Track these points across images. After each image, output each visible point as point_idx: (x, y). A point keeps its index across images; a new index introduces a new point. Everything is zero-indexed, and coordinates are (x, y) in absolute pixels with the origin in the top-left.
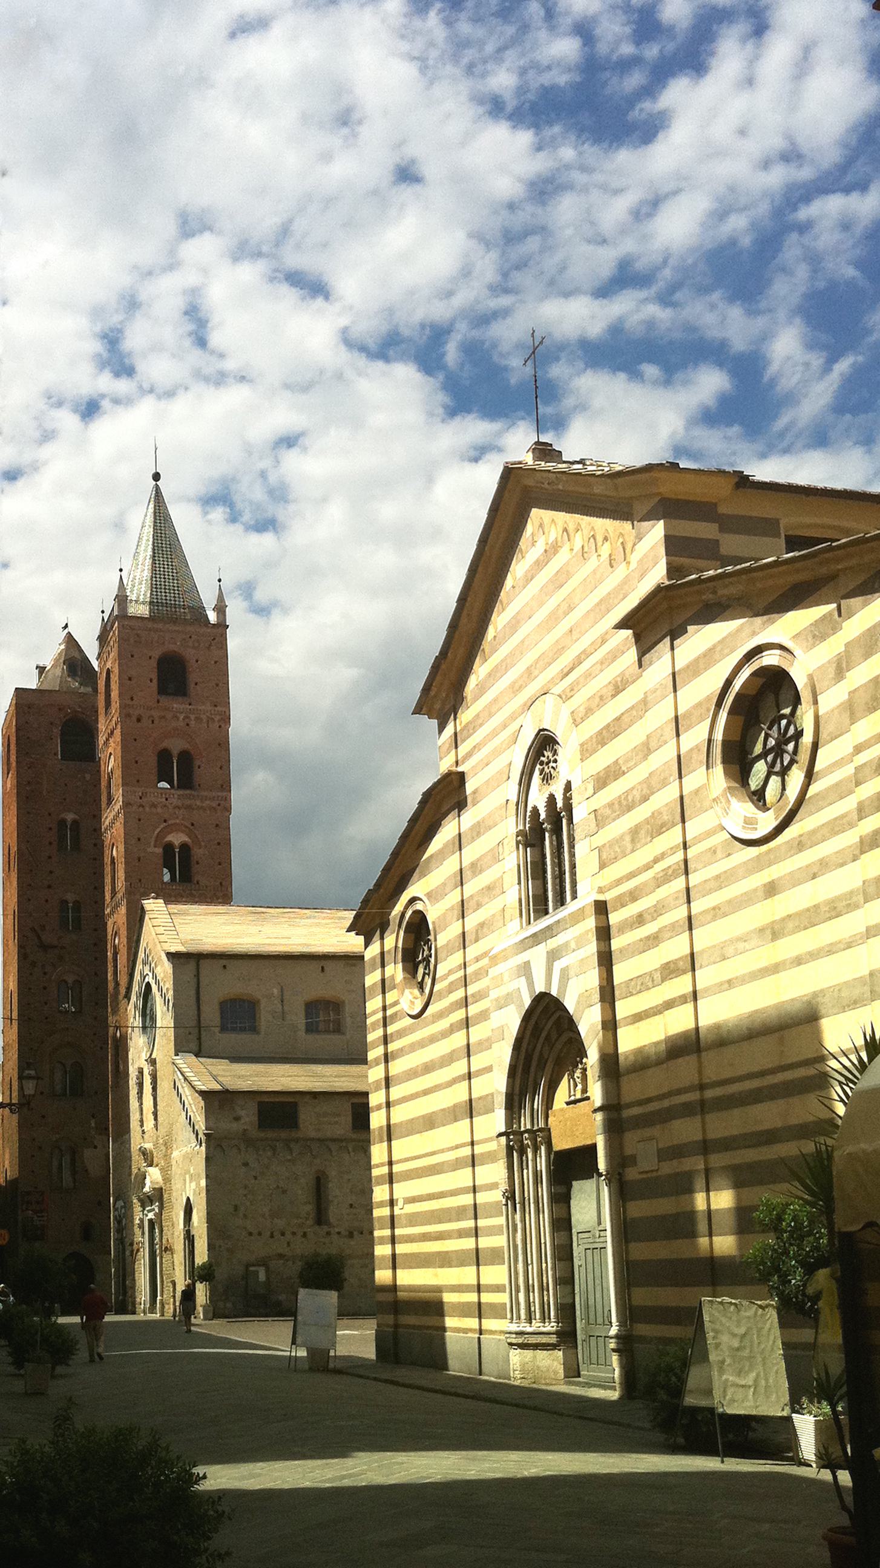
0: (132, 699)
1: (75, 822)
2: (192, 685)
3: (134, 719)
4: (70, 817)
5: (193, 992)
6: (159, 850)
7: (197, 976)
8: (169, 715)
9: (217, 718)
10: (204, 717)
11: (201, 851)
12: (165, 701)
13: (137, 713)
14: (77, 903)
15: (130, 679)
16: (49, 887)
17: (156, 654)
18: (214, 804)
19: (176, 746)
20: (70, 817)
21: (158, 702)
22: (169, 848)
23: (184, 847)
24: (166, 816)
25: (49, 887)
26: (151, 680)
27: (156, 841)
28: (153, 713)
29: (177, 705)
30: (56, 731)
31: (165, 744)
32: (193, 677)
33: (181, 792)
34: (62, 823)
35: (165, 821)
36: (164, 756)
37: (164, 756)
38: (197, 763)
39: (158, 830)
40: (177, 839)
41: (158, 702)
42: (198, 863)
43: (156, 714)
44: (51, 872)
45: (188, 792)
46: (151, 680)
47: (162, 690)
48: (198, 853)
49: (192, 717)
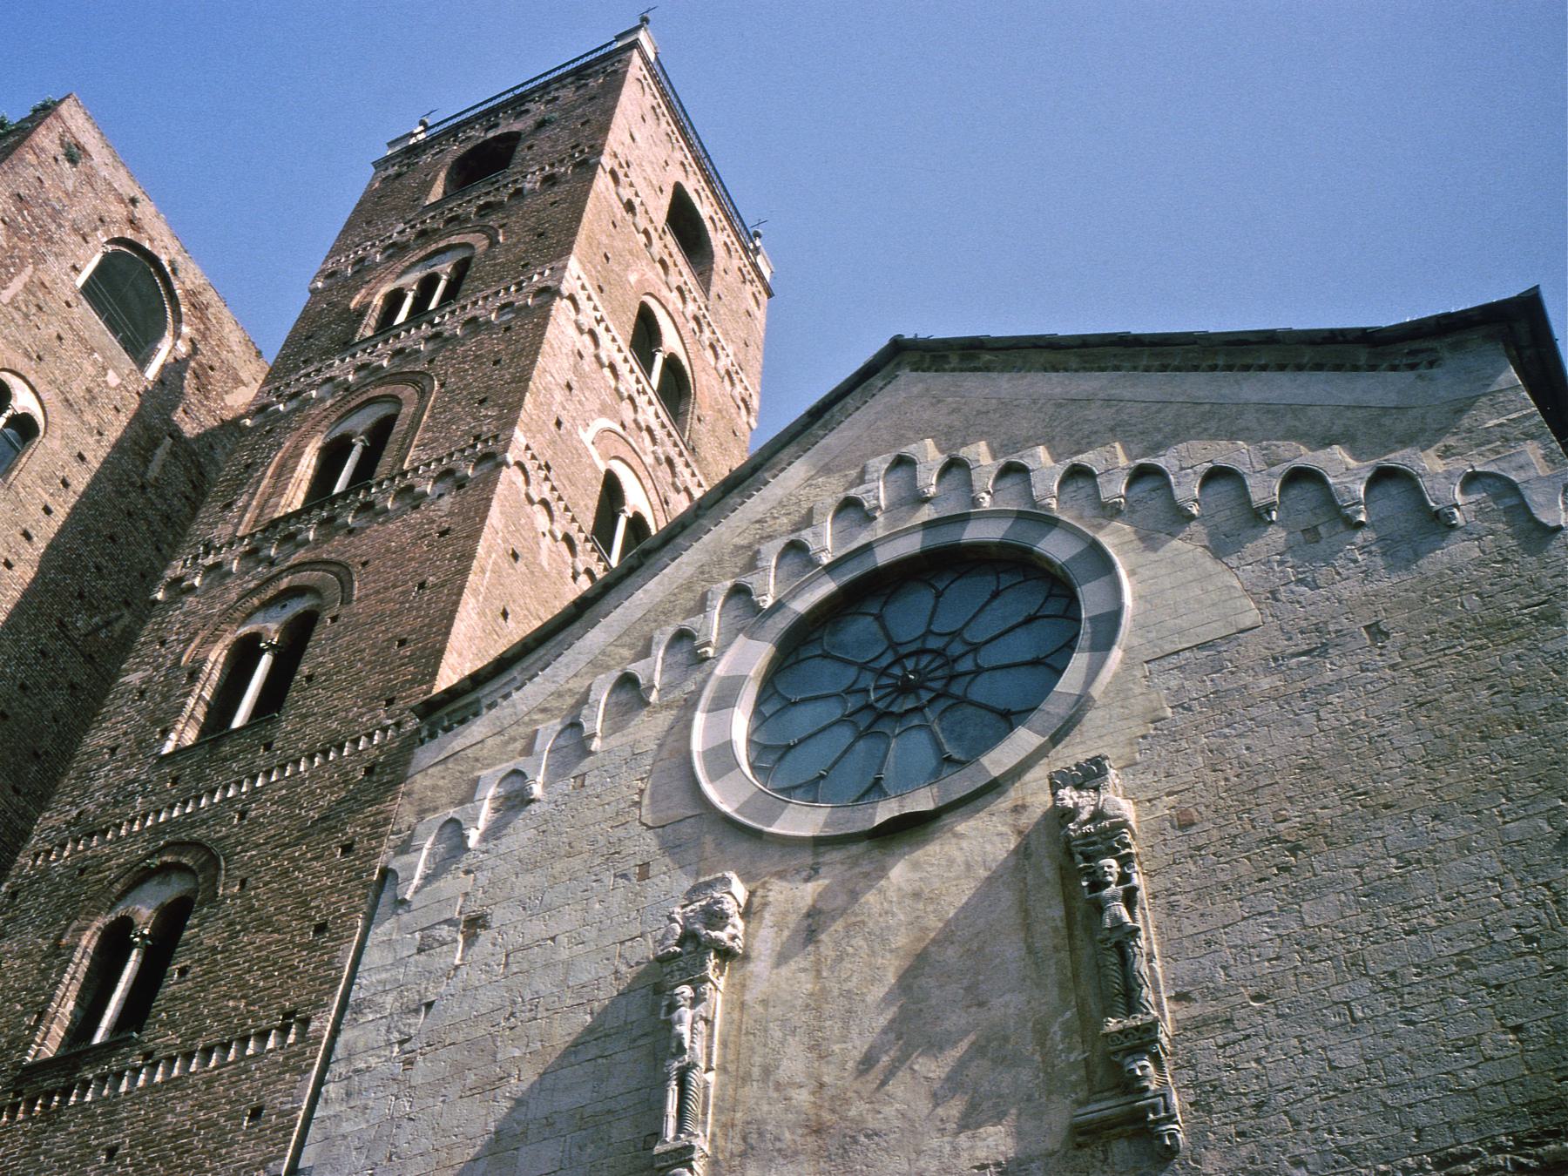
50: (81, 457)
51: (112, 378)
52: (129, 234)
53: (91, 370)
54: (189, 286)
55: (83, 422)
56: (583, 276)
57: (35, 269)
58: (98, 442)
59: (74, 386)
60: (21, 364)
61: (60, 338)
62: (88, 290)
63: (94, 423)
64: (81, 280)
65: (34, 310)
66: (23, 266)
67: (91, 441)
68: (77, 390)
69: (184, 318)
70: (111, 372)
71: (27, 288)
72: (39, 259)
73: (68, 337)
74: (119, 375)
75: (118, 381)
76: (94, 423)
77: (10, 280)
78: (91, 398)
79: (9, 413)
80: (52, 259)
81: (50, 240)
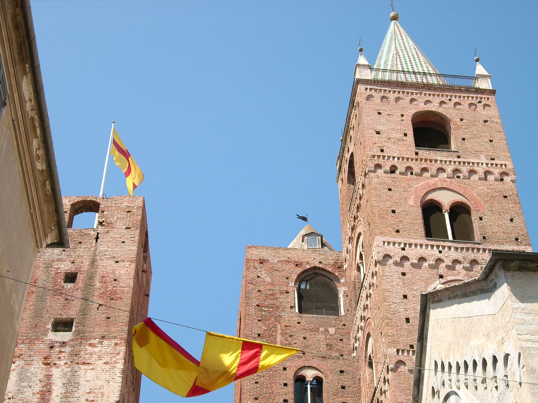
0: (382, 151)
3: (388, 168)
9: (497, 171)
12: (424, 153)
15: (378, 133)
19: (446, 199)
21: (417, 154)
26: (406, 135)
28: (410, 164)
31: (430, 197)
34: (300, 380)
35: (441, 277)
36: (430, 209)
37: (430, 209)
41: (417, 154)
46: (406, 135)
50: (342, 372)
51: (332, 330)
52: (299, 270)
53: (322, 337)
54: (332, 262)
55: (334, 359)
56: (385, 239)
57: (280, 324)
58: (343, 359)
60: (300, 363)
61: (305, 338)
63: (337, 354)
65: (290, 339)
66: (275, 327)
67: (341, 362)
69: (339, 277)
70: (330, 329)
72: (278, 319)
76: (337, 354)
77: (276, 338)
78: (329, 346)
80: (282, 313)
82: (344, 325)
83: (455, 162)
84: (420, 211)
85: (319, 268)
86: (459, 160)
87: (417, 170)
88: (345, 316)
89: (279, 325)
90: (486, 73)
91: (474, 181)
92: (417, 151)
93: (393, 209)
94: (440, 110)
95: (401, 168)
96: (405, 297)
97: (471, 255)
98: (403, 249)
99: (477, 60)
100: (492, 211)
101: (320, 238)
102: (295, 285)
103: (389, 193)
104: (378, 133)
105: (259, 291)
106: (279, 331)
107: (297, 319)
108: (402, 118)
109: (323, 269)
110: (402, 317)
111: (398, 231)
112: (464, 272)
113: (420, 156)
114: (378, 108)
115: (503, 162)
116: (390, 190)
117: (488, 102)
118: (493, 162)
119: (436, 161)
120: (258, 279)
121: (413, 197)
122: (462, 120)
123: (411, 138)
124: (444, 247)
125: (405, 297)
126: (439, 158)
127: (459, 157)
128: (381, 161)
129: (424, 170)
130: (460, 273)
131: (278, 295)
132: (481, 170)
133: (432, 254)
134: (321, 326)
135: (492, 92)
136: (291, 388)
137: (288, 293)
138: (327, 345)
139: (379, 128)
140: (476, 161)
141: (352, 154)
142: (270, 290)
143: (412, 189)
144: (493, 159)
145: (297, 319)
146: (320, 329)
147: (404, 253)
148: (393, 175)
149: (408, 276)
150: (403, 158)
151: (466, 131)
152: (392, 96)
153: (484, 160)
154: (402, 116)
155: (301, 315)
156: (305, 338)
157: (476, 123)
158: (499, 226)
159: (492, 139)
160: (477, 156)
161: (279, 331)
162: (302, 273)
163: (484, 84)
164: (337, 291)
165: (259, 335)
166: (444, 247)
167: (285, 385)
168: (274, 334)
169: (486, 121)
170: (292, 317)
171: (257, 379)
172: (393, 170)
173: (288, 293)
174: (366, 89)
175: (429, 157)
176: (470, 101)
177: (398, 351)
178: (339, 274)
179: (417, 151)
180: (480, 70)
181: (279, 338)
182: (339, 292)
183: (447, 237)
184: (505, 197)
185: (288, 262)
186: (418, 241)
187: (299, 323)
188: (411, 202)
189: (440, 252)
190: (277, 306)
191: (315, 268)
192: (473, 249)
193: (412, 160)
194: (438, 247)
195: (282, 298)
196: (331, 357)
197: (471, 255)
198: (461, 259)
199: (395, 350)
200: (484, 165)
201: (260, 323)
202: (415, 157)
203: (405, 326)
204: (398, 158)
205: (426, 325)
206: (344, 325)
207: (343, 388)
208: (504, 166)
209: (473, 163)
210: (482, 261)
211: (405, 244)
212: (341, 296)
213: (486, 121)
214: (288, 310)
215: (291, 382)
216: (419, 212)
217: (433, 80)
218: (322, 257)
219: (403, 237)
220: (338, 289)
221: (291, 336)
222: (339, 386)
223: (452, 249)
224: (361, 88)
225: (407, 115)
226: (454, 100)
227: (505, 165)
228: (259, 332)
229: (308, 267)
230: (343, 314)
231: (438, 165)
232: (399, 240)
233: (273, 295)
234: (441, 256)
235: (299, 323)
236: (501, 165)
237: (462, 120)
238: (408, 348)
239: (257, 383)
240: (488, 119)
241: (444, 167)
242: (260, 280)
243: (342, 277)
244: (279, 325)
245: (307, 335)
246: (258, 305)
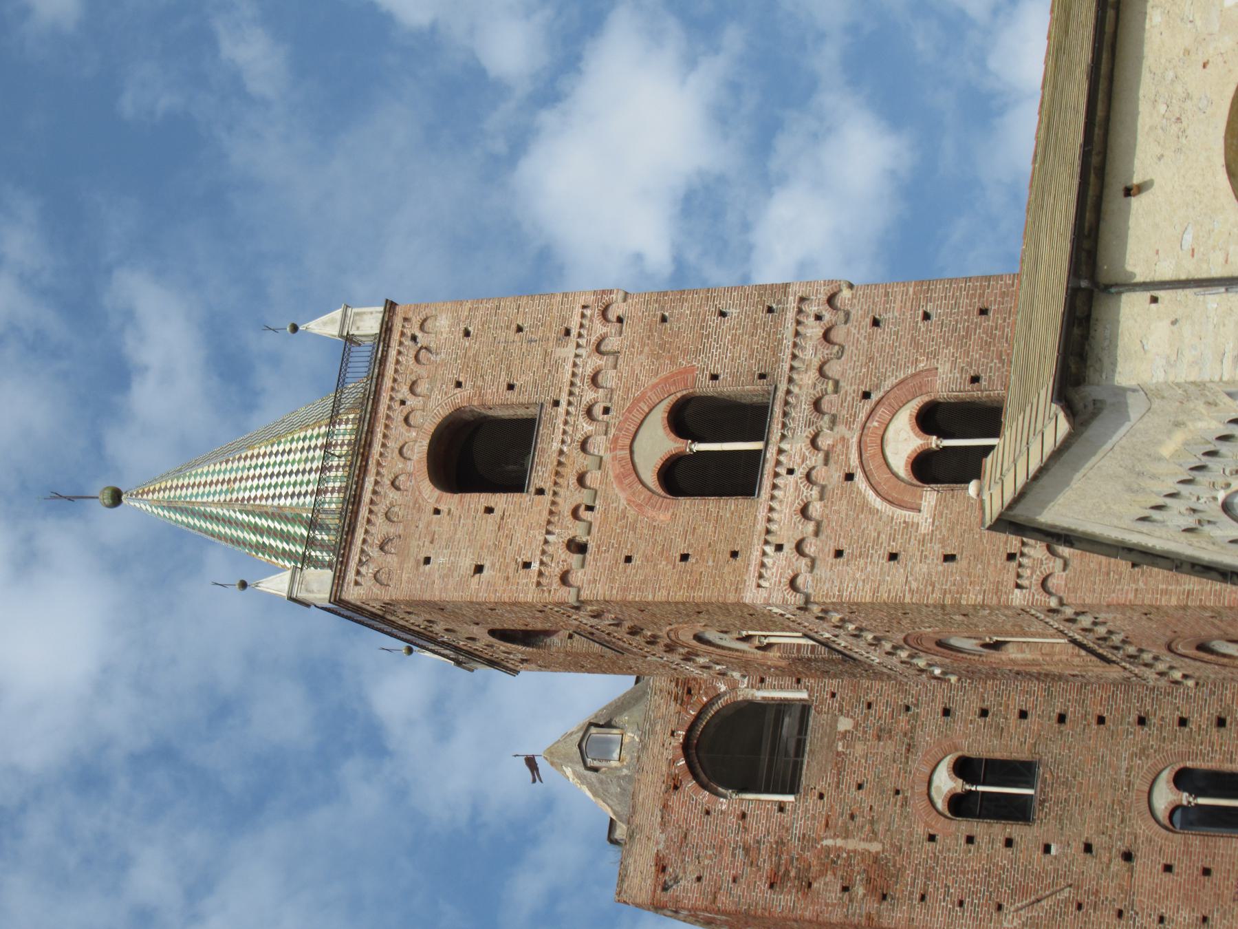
0: (527, 565)
1: (964, 768)
2: (512, 397)
3: (575, 558)
4: (945, 783)
5: (1214, 300)
6: (930, 497)
7: (1154, 286)
8: (578, 461)
9: (599, 328)
10: (592, 363)
11: (944, 368)
12: (540, 476)
13: (563, 554)
14: (1183, 779)
15: (479, 569)
16: (1128, 857)
17: (430, 493)
18: (814, 331)
19: (658, 443)
20: (945, 783)
21: (540, 492)
22: (926, 468)
23: (929, 419)
24: (836, 475)
25: (1128, 857)
26: (489, 510)
27: (900, 505)
28: (565, 508)
29: (550, 444)
30: (728, 803)
31: (650, 476)
32: (491, 396)
33: (776, 431)
34: (959, 805)
35: (849, 477)
36: (678, 478)
37: (678, 478)
38: (705, 387)
39: (877, 503)
40: (904, 441)
41: (540, 492)
42: (975, 379)
43: (571, 496)
44: (1088, 848)
45: (778, 410)
46: (489, 510)
47: (512, 480)
48: (947, 384)
49: (589, 395)
50: (946, 712)
51: (845, 724)
52: (690, 784)
53: (860, 748)
54: (674, 708)
55: (913, 727)
57: (822, 839)
59: (888, 752)
61: (860, 787)
62: (792, 787)
64: (790, 798)
65: (859, 820)
66: (828, 850)
67: (922, 711)
68: (888, 748)
69: (712, 694)
71: (847, 835)
73: (850, 780)
74: (836, 721)
75: (841, 718)
76: (903, 718)
77: (855, 851)
79: (968, 787)
81: (781, 843)
82: (833, 695)
83: (568, 413)
84: (685, 503)
85: (687, 738)
86: (563, 403)
87: (584, 497)
88: (810, 690)
89: (825, 843)
90: (337, 314)
91: (620, 379)
92: (532, 489)
93: (678, 558)
94: (430, 427)
95: (577, 531)
96: (893, 557)
97: (802, 410)
98: (779, 548)
99: (295, 328)
100: (697, 352)
101: (593, 730)
102: (725, 797)
103: (637, 561)
104: (479, 569)
105: (734, 881)
106: (839, 842)
107: (812, 799)
108: (444, 514)
109: (690, 731)
110: (940, 568)
111: (734, 554)
112: (841, 429)
113: (548, 486)
114: (410, 564)
115: (578, 310)
116: (628, 559)
117: (416, 321)
118: (574, 332)
119: (561, 452)
120: (704, 882)
121: (650, 512)
122: (459, 385)
123: (500, 501)
124: (778, 463)
125: (893, 557)
126: (556, 446)
127: (556, 403)
128: (555, 570)
129: (581, 480)
130: (843, 439)
131: (749, 838)
132: (592, 363)
133: (790, 491)
134: (831, 744)
135: (391, 306)
136: (979, 828)
137: (744, 816)
138: (879, 738)
139: (468, 563)
140: (568, 368)
141: (493, 633)
142: (734, 855)
143: (631, 513)
144: (568, 332)
145: (812, 799)
146: (840, 749)
147: (789, 548)
148: (592, 547)
149: (843, 544)
150: (549, 522)
151: (488, 378)
152: (381, 528)
153: (569, 351)
154: (437, 512)
155: (802, 790)
156: (860, 787)
157: (470, 354)
158: (735, 340)
159: (514, 327)
160: (557, 365)
161: (839, 842)
162: (695, 776)
163: (369, 323)
164: (745, 701)
165: (845, 889)
166: (778, 463)
167: (970, 840)
168: (845, 855)
169: (467, 333)
170: (807, 810)
171: (953, 904)
172: (578, 548)
173: (744, 816)
174: (357, 583)
175: (552, 466)
176: (408, 360)
177: (1018, 586)
178: (706, 694)
179: (532, 489)
180: (326, 326)
181: (852, 844)
182: (749, 697)
183: (758, 452)
184: (664, 319)
185: (665, 806)
186: (762, 514)
187: (821, 796)
188: (663, 517)
189: (791, 472)
190: (777, 843)
191: (686, 746)
192: (786, 403)
193: (553, 503)
194: (776, 475)
195: (758, 827)
196: (909, 734)
197: (802, 410)
198: (811, 431)
199: (1017, 591)
200: (579, 351)
201: (815, 885)
202: (548, 497)
203: (961, 563)
204: (548, 532)
205: (1043, 527)
206: (833, 695)
207: (984, 713)
208: (588, 312)
209: (574, 375)
210: (819, 389)
211: (766, 542)
212: (760, 695)
213: (467, 333)
214: (786, 818)
215: (964, 826)
216: (686, 505)
217: (345, 432)
218: (658, 728)
219: (749, 545)
220: (740, 699)
221: (852, 817)
222: (981, 721)
223: (785, 446)
224: (352, 594)
225: (438, 500)
226: (404, 391)
227: (584, 307)
228: (839, 888)
229: (682, 762)
230: (804, 695)
231: (572, 450)
232: (756, 554)
233: (747, 850)
234: (800, 472)
235: (821, 796)
236: (583, 316)
237: (459, 385)
238: (1014, 564)
239: (961, 903)
240: (462, 327)
241: (579, 436)
242: (706, 875)
243: (715, 688)
244: (825, 843)
245: (850, 780)
246: (772, 886)
